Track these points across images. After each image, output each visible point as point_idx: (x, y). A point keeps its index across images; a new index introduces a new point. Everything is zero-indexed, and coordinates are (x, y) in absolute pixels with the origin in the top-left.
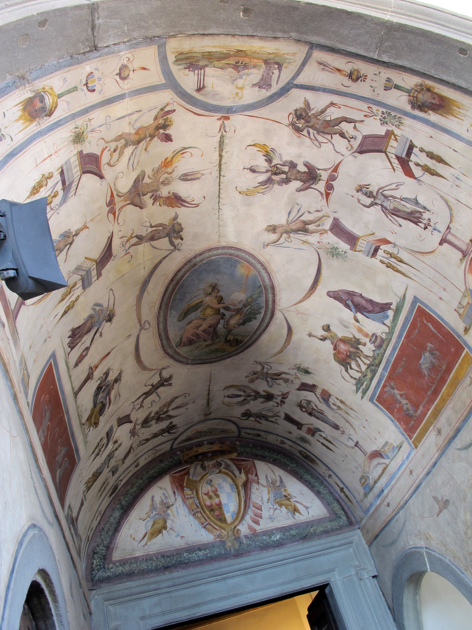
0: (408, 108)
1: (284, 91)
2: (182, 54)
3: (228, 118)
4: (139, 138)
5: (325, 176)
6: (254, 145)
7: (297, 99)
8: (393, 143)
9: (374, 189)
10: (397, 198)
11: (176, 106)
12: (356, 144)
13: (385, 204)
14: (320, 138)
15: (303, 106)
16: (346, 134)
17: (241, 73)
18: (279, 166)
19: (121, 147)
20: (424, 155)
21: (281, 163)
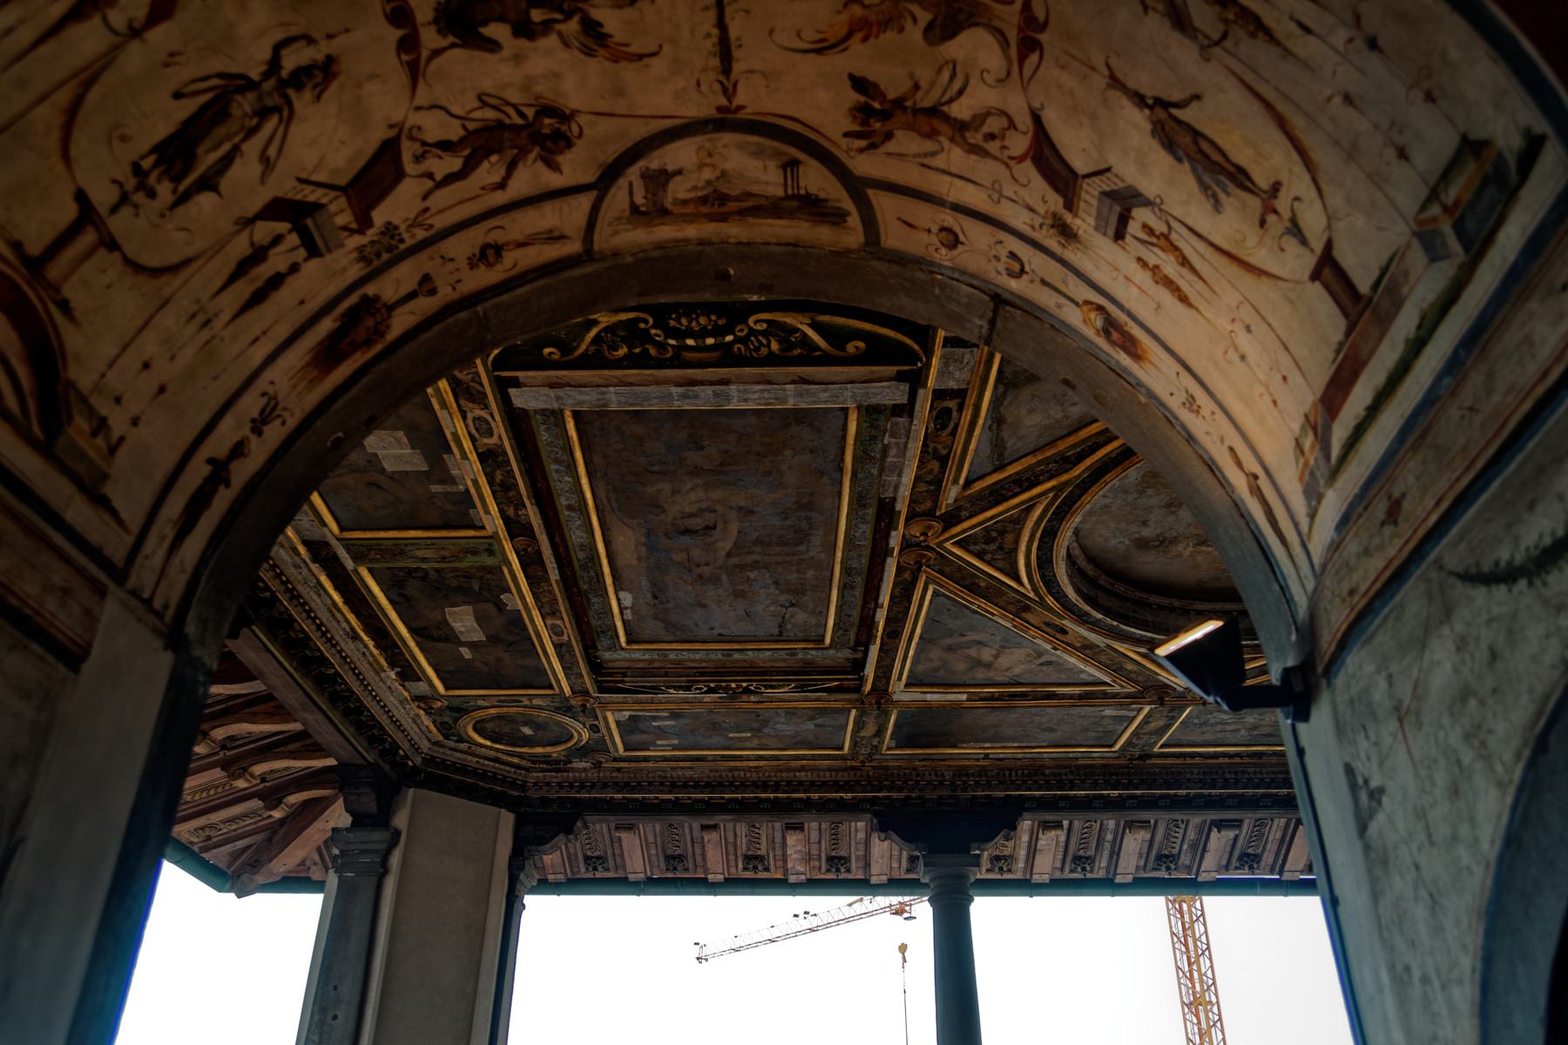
0: (370, 290)
1: (610, 174)
2: (834, 224)
3: (720, 109)
4: (932, 119)
5: (430, 38)
6: (641, 57)
7: (576, 166)
8: (344, 219)
9: (302, 101)
10: (245, 139)
11: (844, 142)
12: (408, 150)
13: (251, 96)
14: (490, 114)
15: (560, 158)
16: (439, 152)
17: (710, 190)
18: (558, 16)
19: (976, 130)
20: (282, 268)
21: (558, 27)
